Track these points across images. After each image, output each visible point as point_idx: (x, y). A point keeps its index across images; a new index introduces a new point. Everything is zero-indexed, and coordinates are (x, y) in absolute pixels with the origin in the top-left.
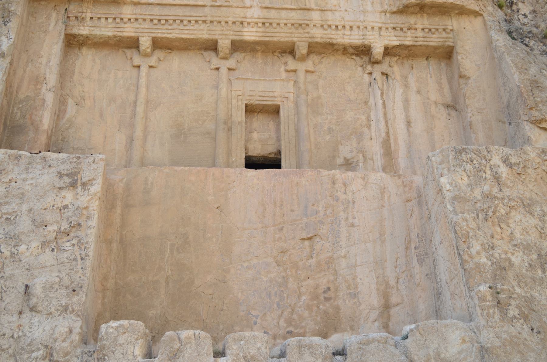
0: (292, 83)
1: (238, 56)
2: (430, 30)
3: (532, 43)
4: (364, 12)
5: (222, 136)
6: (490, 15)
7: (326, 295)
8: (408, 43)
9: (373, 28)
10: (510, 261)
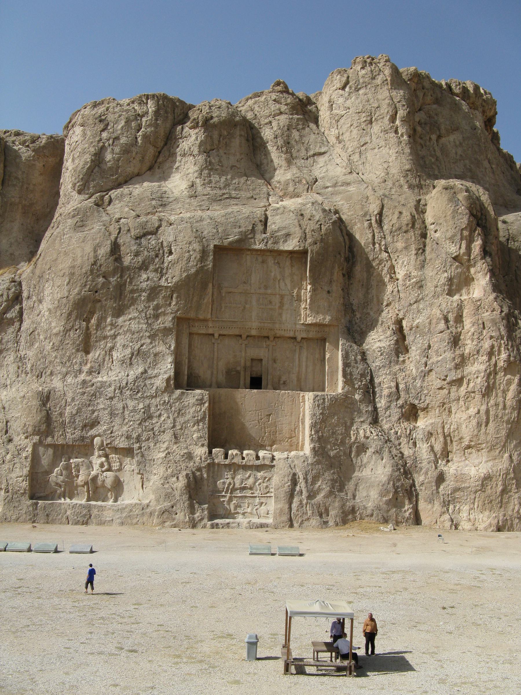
1: (248, 338)
5: (242, 373)
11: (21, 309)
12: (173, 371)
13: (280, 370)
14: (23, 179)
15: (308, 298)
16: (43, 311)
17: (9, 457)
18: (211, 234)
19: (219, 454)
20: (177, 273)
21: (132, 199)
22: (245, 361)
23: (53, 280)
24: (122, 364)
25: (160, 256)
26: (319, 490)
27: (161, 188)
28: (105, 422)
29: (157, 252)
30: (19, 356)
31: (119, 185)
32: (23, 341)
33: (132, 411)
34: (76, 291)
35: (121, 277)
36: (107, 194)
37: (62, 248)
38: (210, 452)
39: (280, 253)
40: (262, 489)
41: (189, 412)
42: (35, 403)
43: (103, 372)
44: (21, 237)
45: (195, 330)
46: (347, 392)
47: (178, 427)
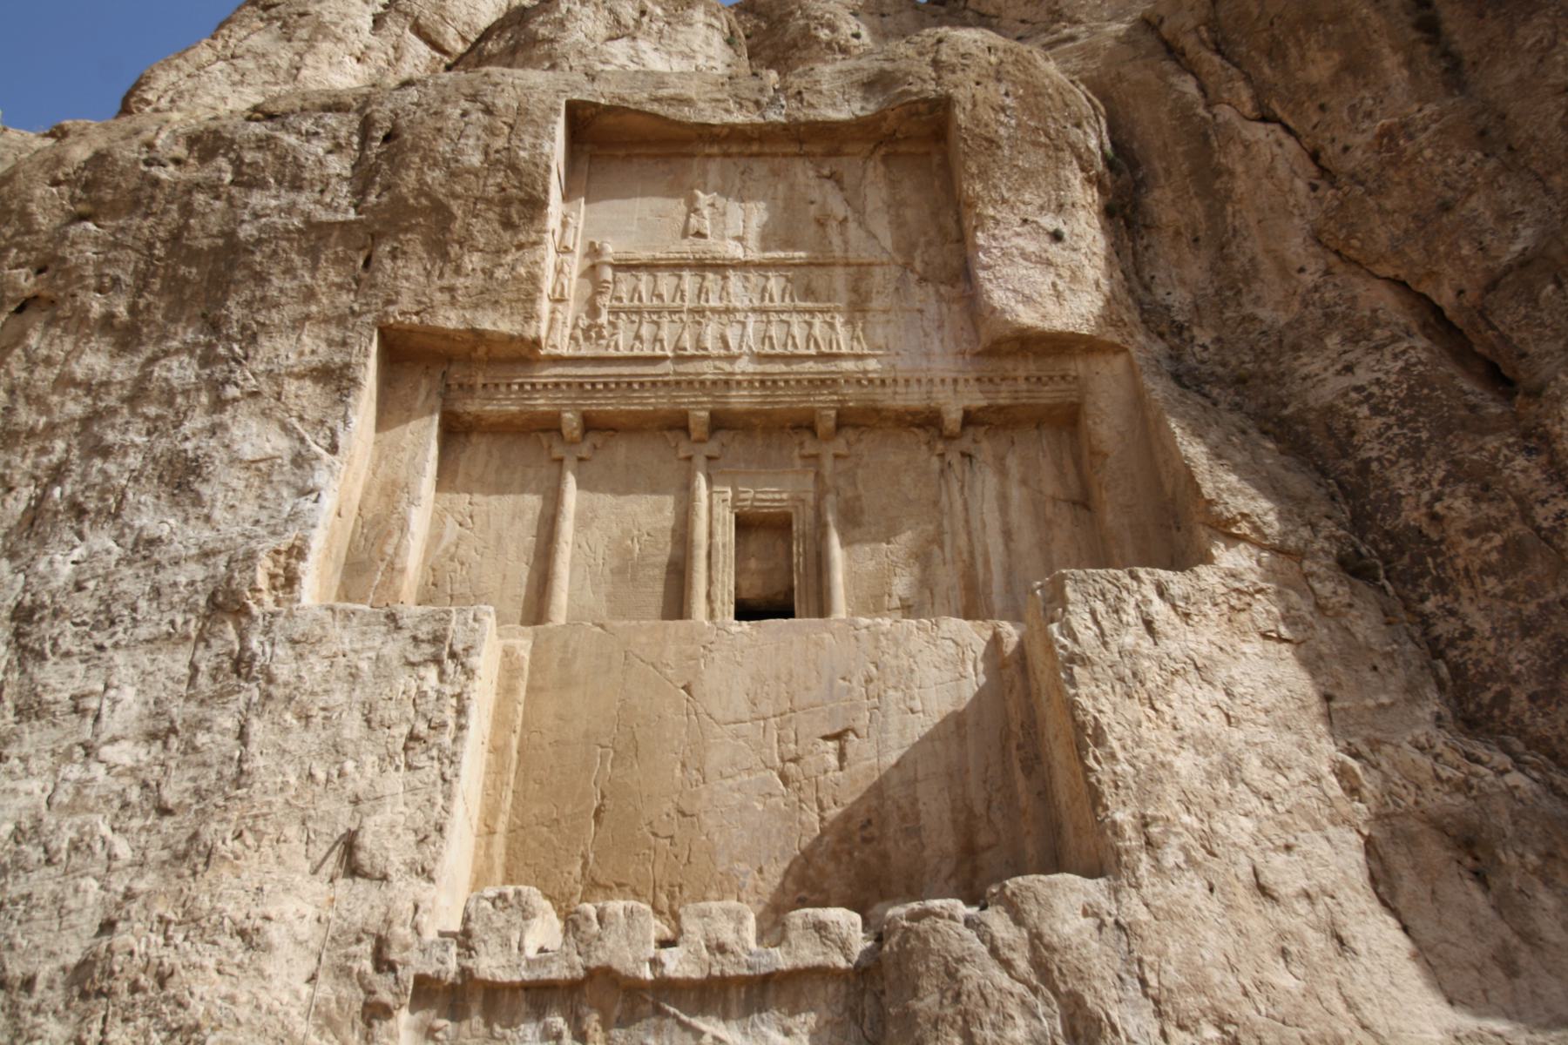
0: (811, 476)
1: (723, 436)
2: (1039, 379)
3: (1215, 392)
4: (928, 355)
6: (1142, 348)
7: (865, 833)
8: (1002, 402)
9: (943, 381)
45: (472, 406)
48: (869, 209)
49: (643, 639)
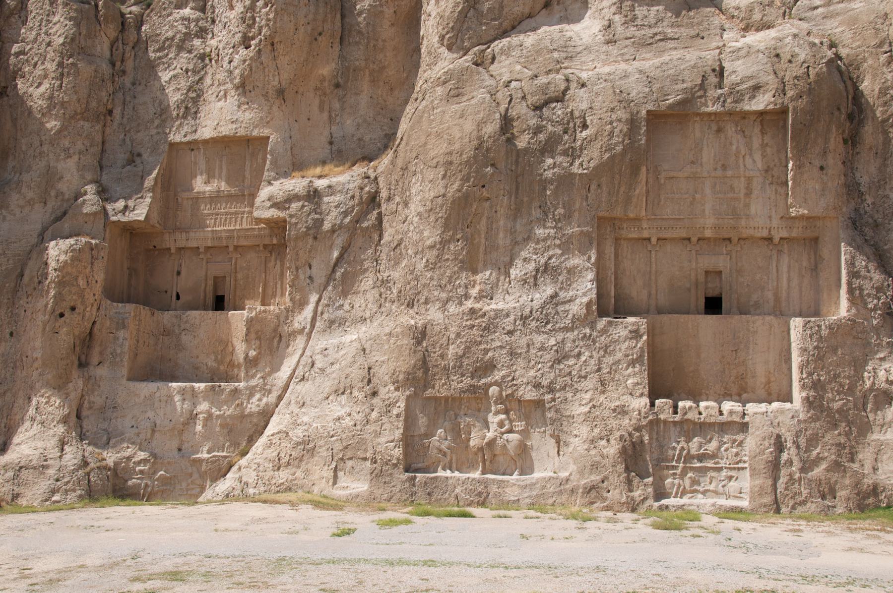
1: (701, 242)
10: (819, 380)
11: (380, 214)
12: (595, 292)
13: (748, 285)
14: (368, 33)
15: (789, 179)
16: (411, 217)
17: (374, 415)
18: (641, 95)
19: (665, 407)
20: (596, 154)
21: (524, 51)
22: (696, 275)
23: (422, 173)
24: (523, 285)
25: (570, 132)
26: (819, 460)
27: (564, 33)
28: (503, 365)
29: (566, 126)
30: (380, 278)
31: (505, 34)
32: (385, 257)
33: (540, 349)
34: (456, 186)
35: (517, 162)
36: (488, 48)
37: (432, 128)
38: (652, 405)
39: (745, 115)
40: (730, 457)
41: (620, 349)
42: (407, 341)
43: (498, 296)
44: (371, 115)
45: (624, 233)
46: (855, 315)
47: (605, 370)
48: (754, 148)
49: (682, 320)
